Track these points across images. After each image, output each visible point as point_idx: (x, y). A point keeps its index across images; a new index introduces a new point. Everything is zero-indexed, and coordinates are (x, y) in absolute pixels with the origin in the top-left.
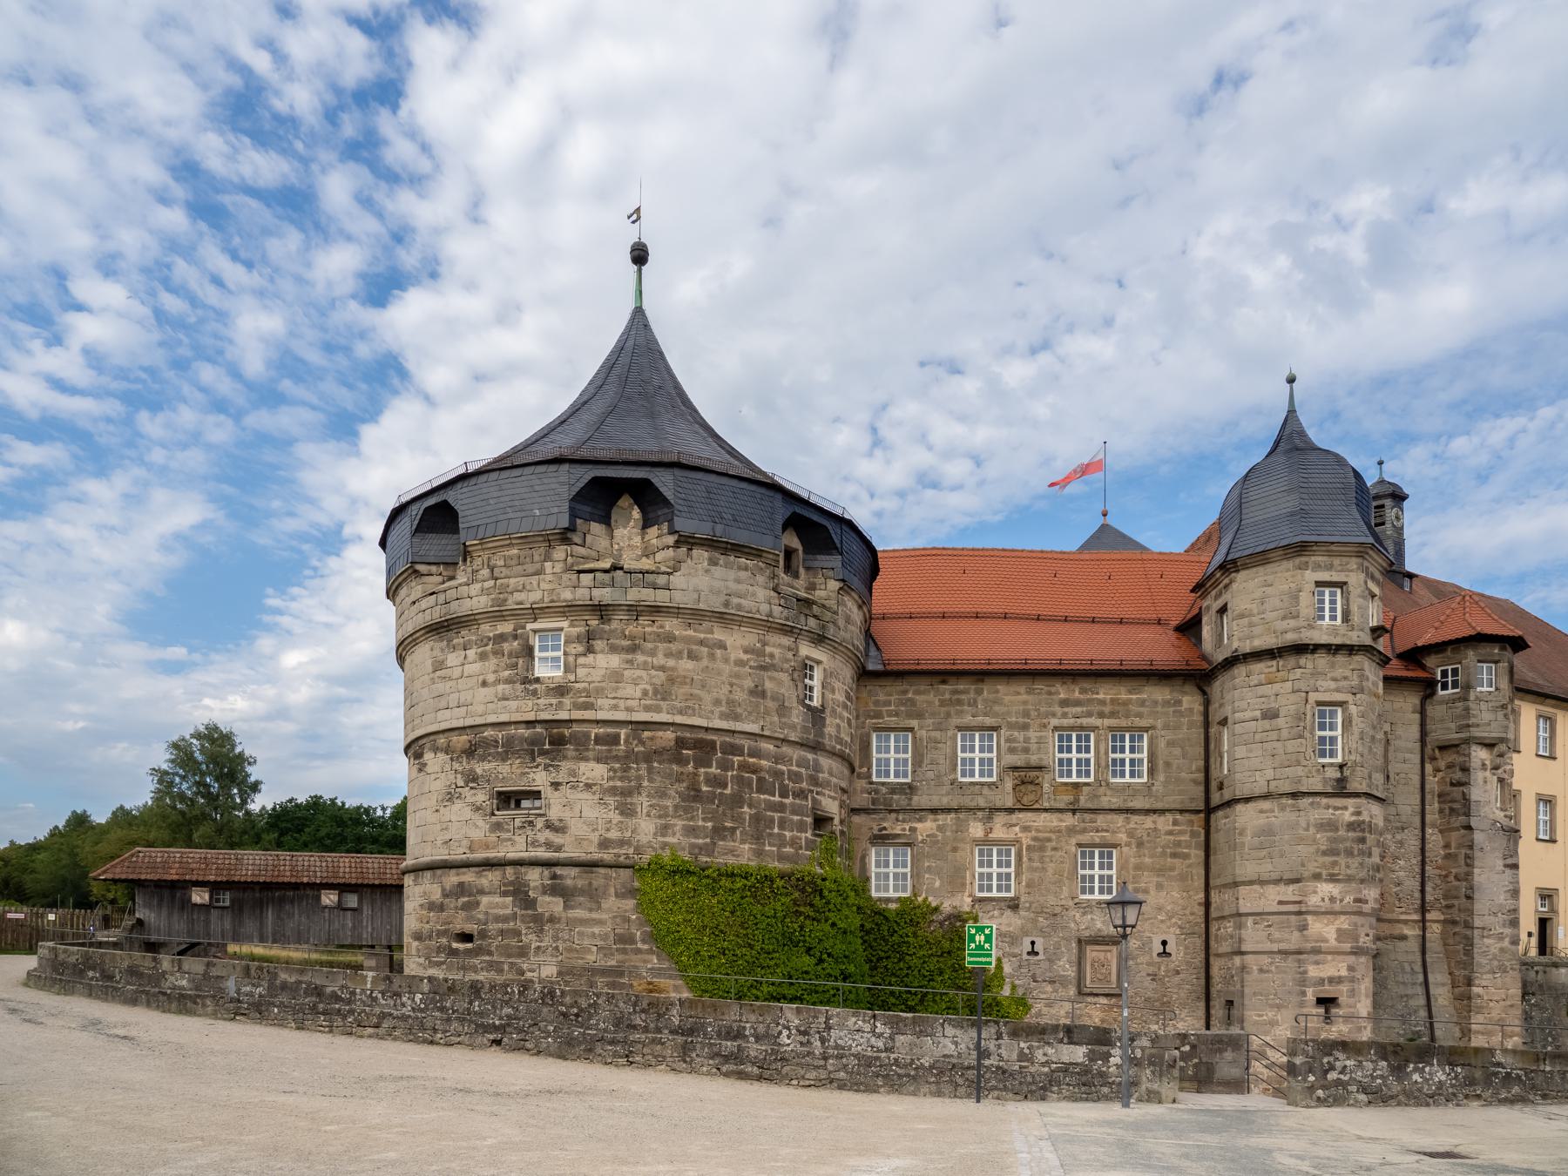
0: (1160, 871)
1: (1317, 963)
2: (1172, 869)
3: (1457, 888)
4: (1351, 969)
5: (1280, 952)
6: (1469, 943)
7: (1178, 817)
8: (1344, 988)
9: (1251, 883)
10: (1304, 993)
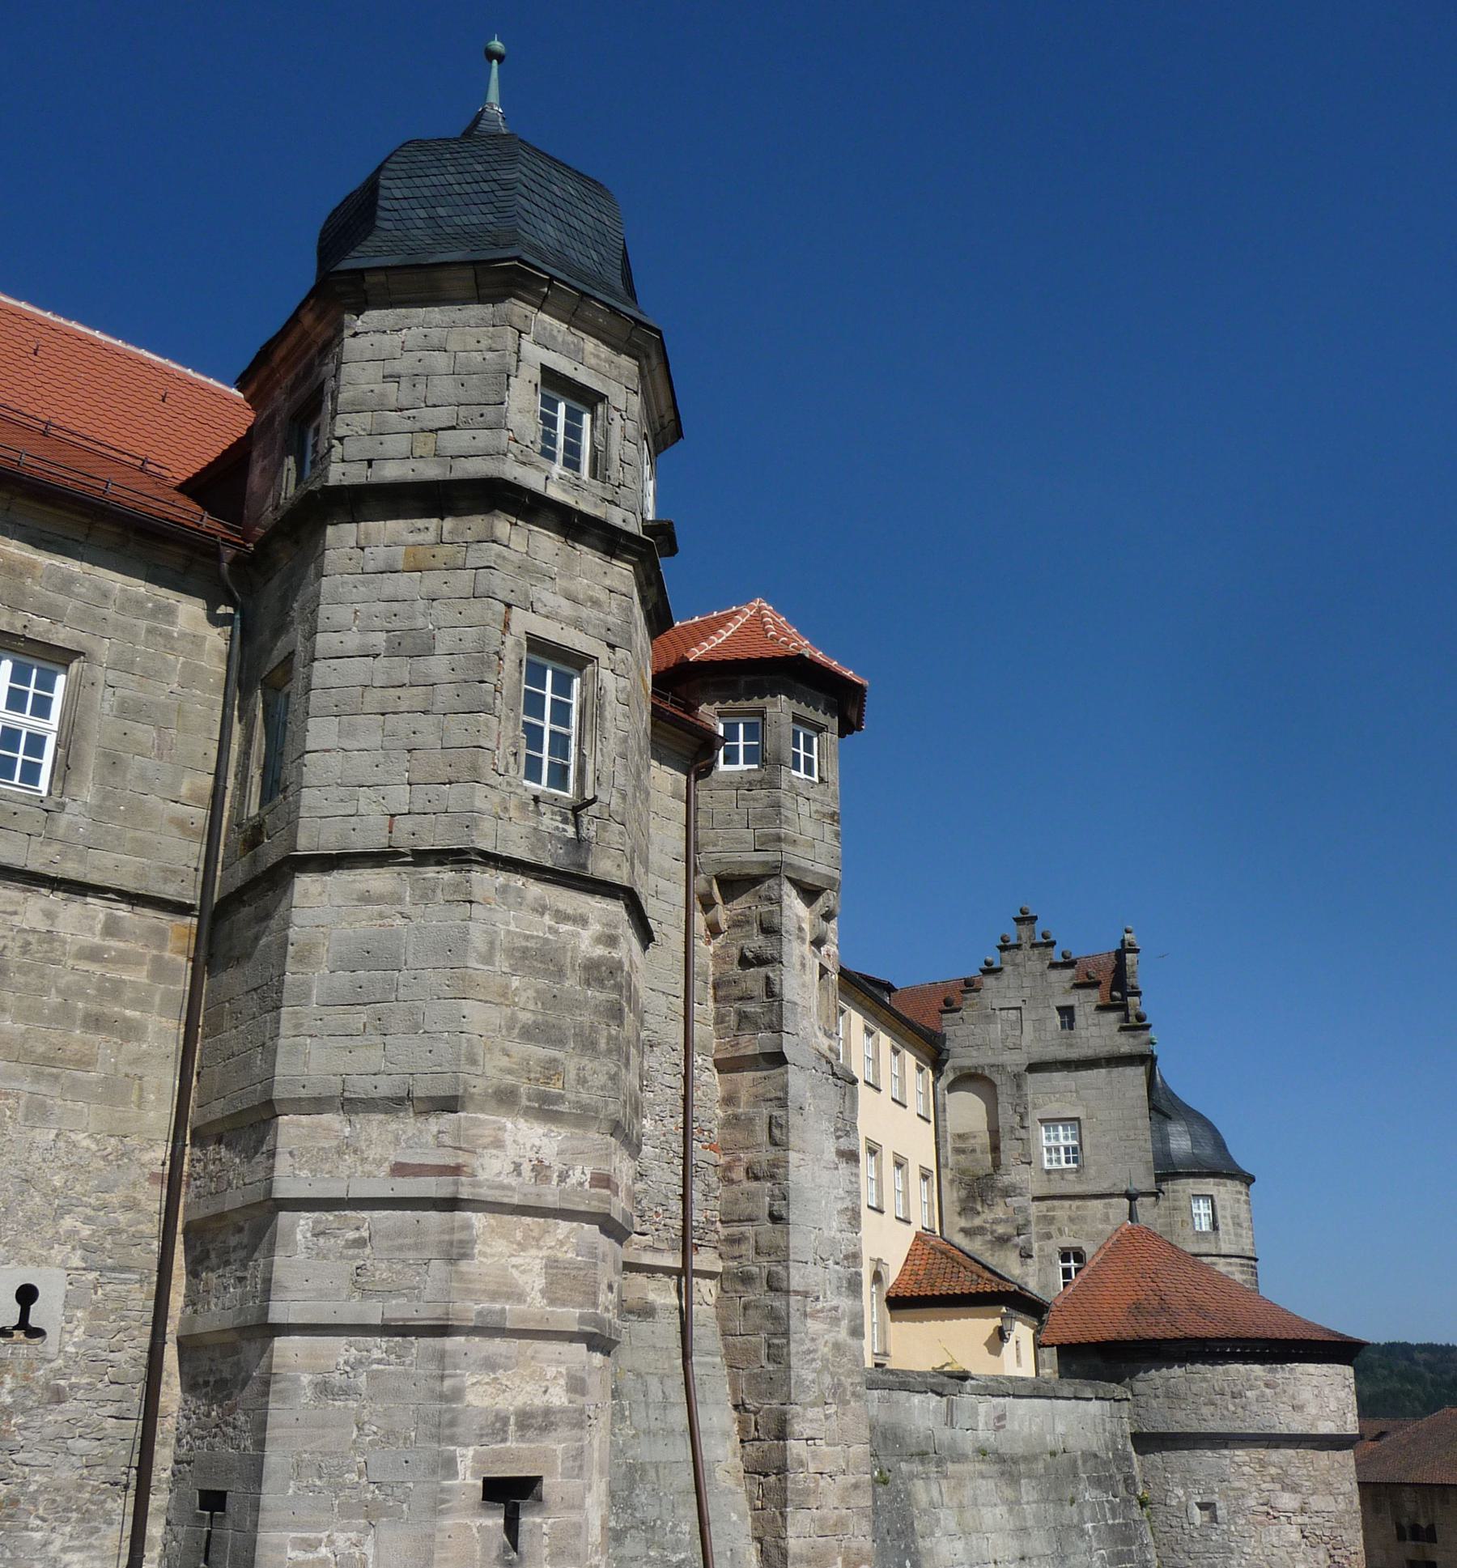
0: (46, 1064)
1: (490, 1364)
2: (84, 1062)
3: (750, 1196)
4: (576, 1386)
5: (387, 1329)
6: (779, 1325)
7: (123, 911)
8: (557, 1445)
9: (318, 1105)
10: (449, 1465)
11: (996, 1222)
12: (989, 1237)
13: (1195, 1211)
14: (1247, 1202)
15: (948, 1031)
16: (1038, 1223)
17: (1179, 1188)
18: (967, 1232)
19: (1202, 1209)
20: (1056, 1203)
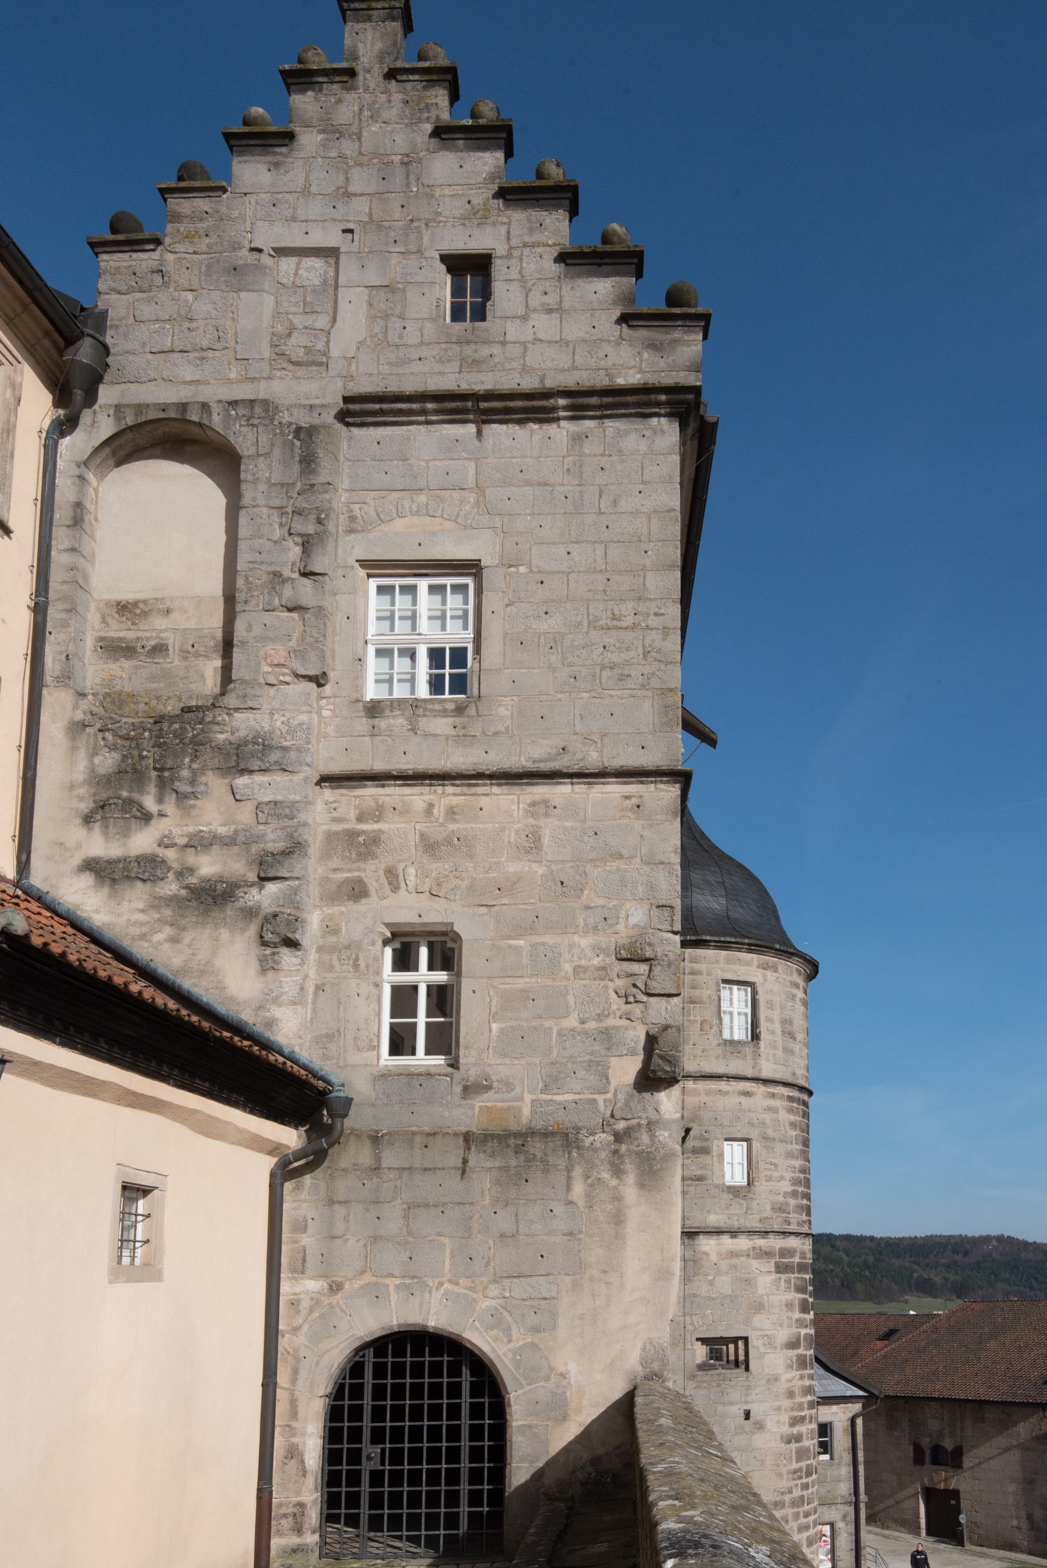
11: (199, 843)
12: (171, 887)
13: (725, 1006)
14: (805, 1003)
15: (116, 306)
16: (327, 854)
17: (702, 967)
18: (104, 872)
19: (736, 1003)
20: (392, 794)
